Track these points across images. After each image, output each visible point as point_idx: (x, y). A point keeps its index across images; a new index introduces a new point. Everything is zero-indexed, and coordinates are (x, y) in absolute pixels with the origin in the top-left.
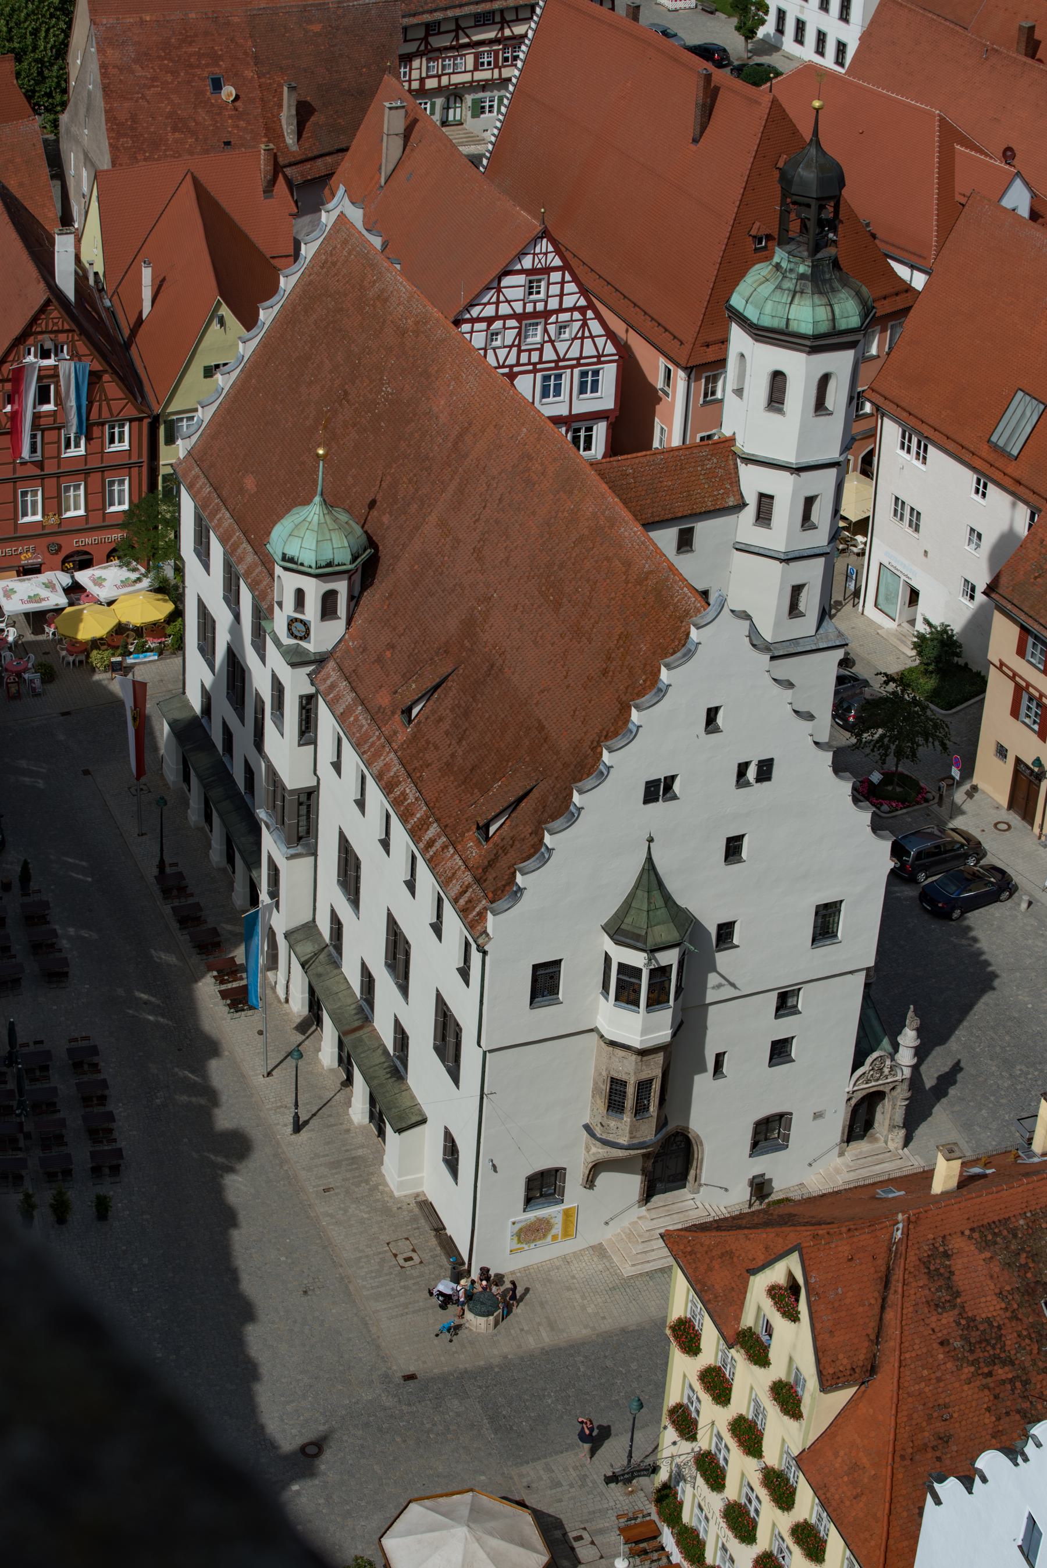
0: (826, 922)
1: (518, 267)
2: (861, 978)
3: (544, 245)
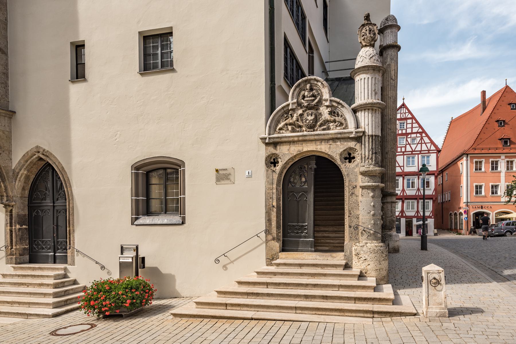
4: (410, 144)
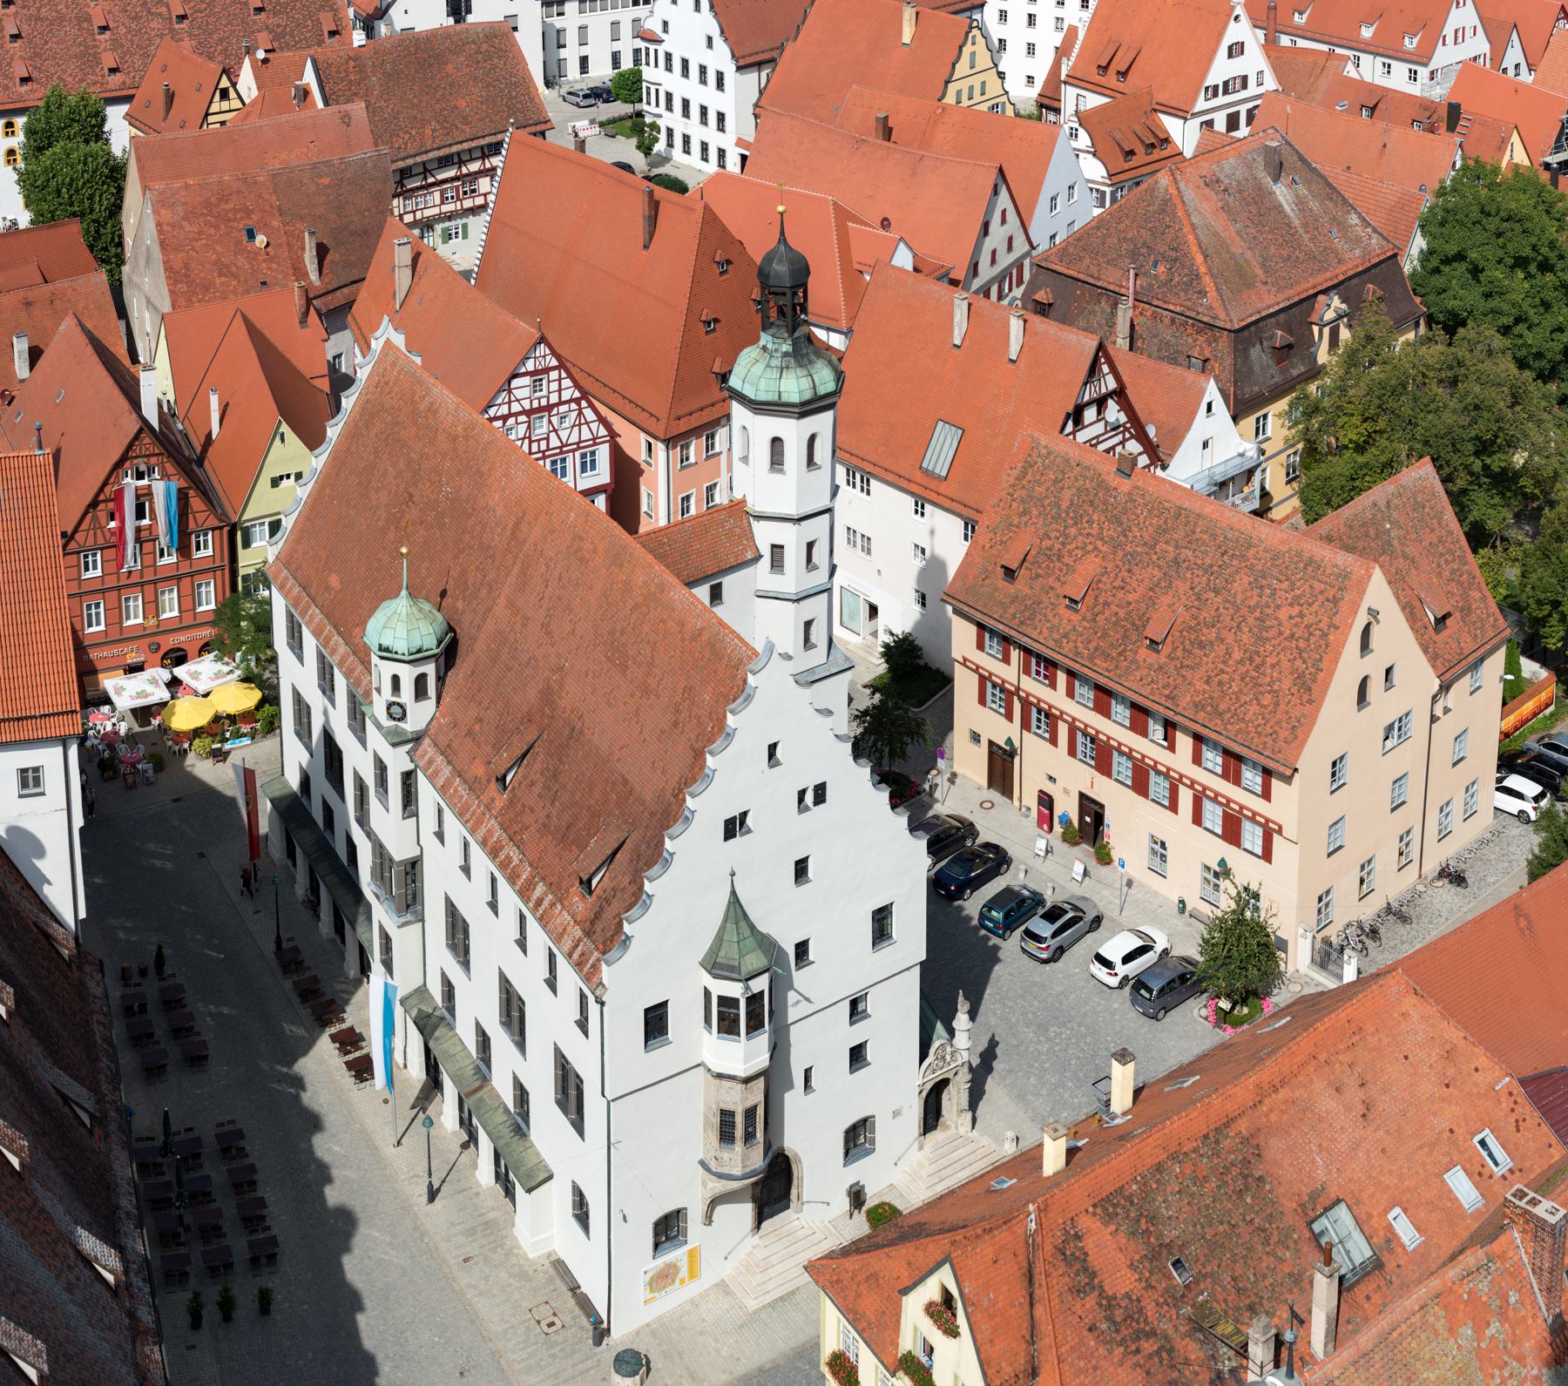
0: (881, 922)
1: (523, 370)
3: (542, 349)
4: (555, 431)
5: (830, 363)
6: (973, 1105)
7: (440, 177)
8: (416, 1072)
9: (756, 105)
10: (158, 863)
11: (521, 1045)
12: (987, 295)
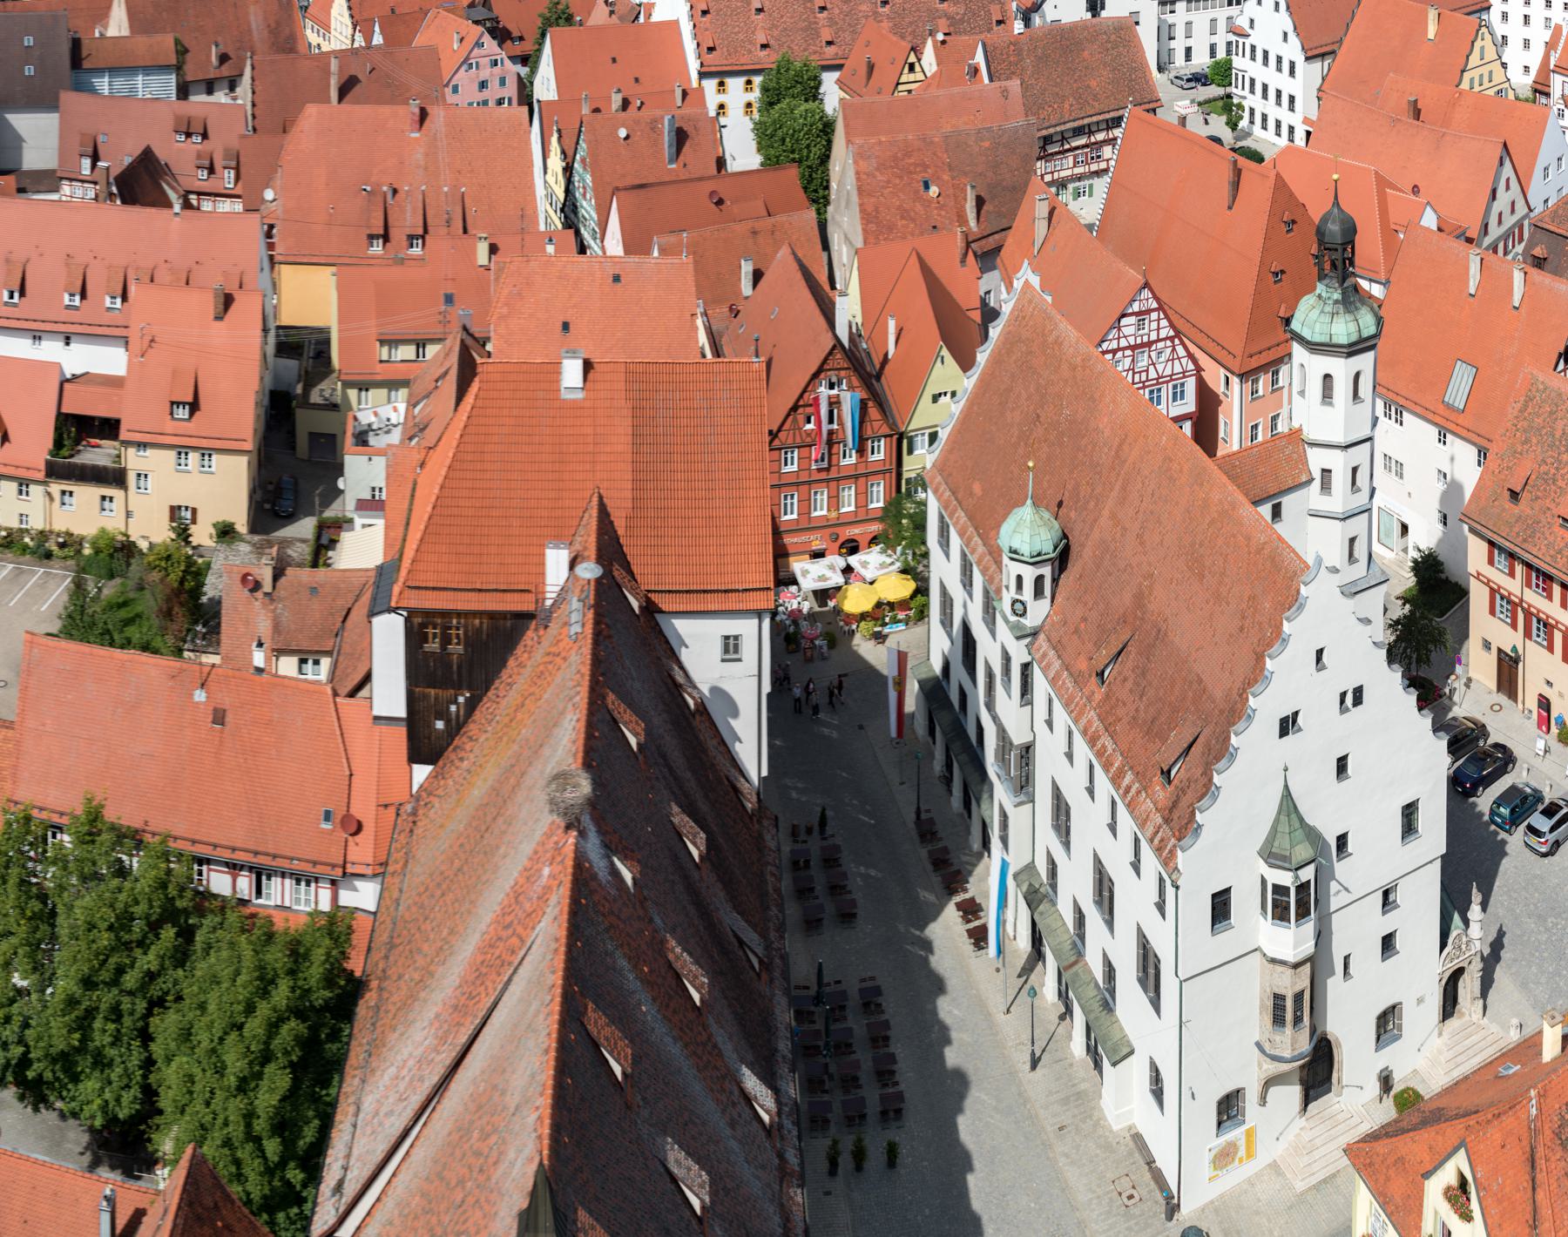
2: (1438, 864)
5: (1372, 309)
6: (1484, 994)
7: (1074, 144)
8: (1024, 943)
9: (1319, 90)
10: (826, 731)
11: (1110, 923)
12: (1495, 251)
